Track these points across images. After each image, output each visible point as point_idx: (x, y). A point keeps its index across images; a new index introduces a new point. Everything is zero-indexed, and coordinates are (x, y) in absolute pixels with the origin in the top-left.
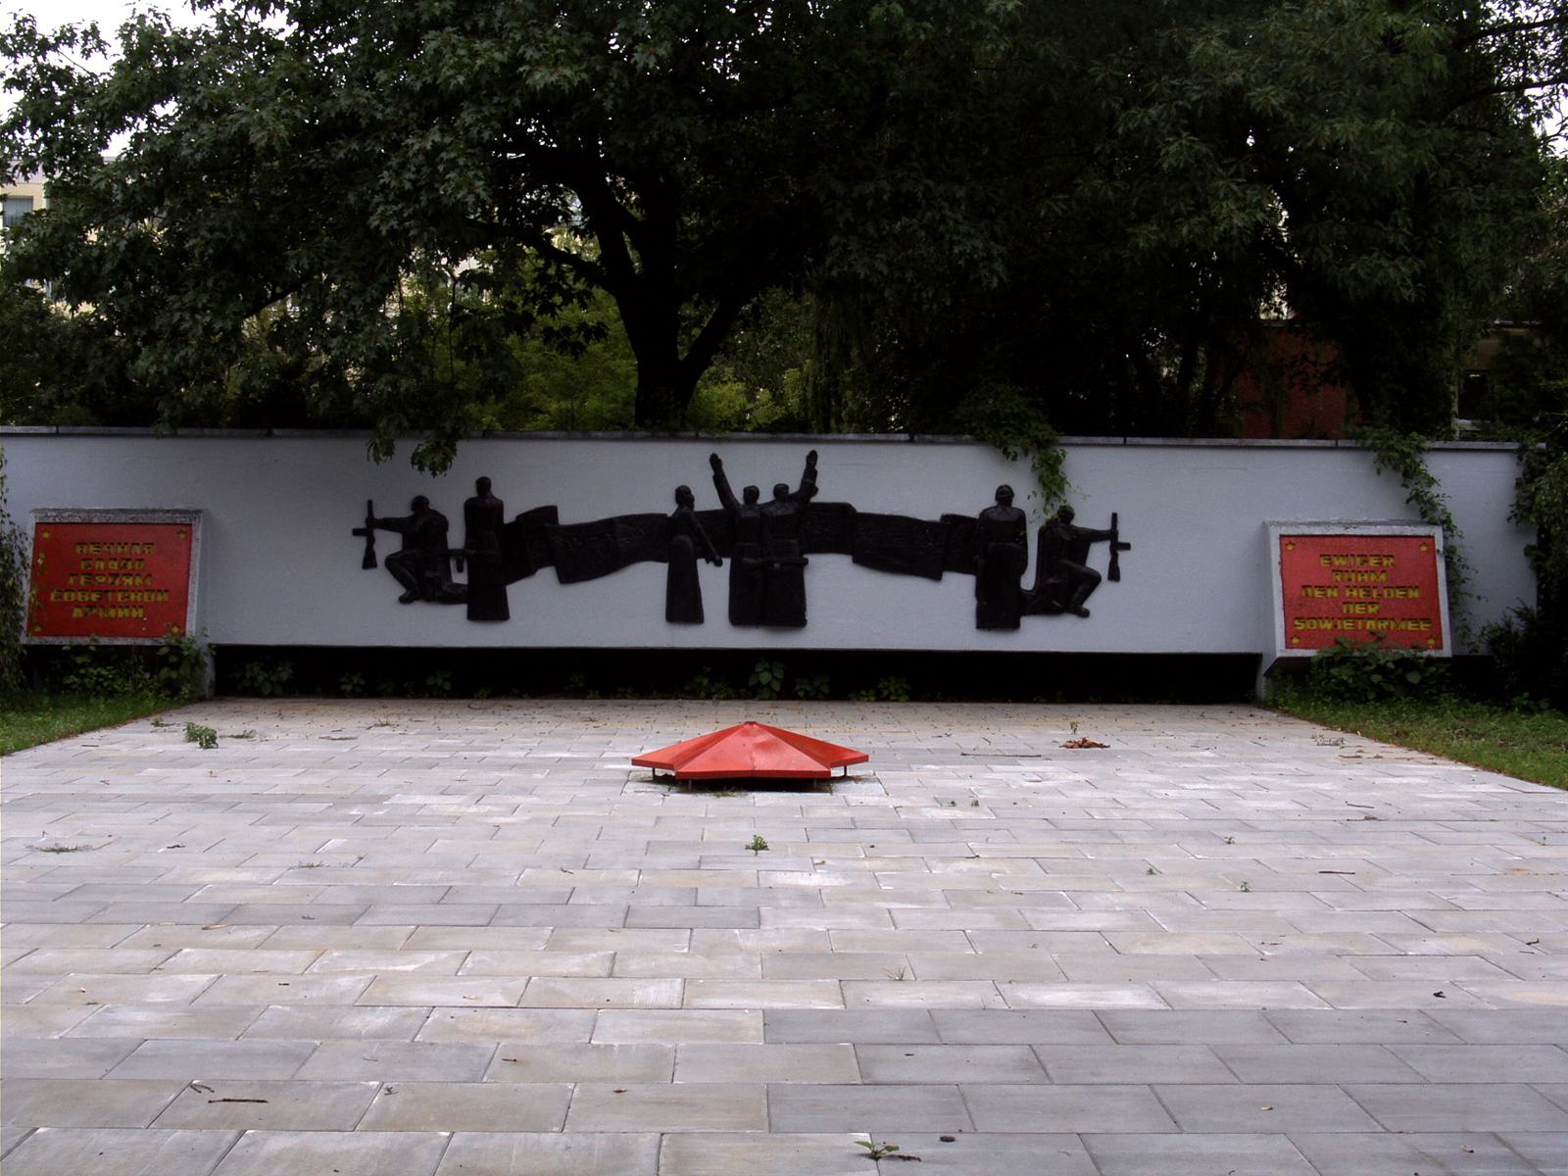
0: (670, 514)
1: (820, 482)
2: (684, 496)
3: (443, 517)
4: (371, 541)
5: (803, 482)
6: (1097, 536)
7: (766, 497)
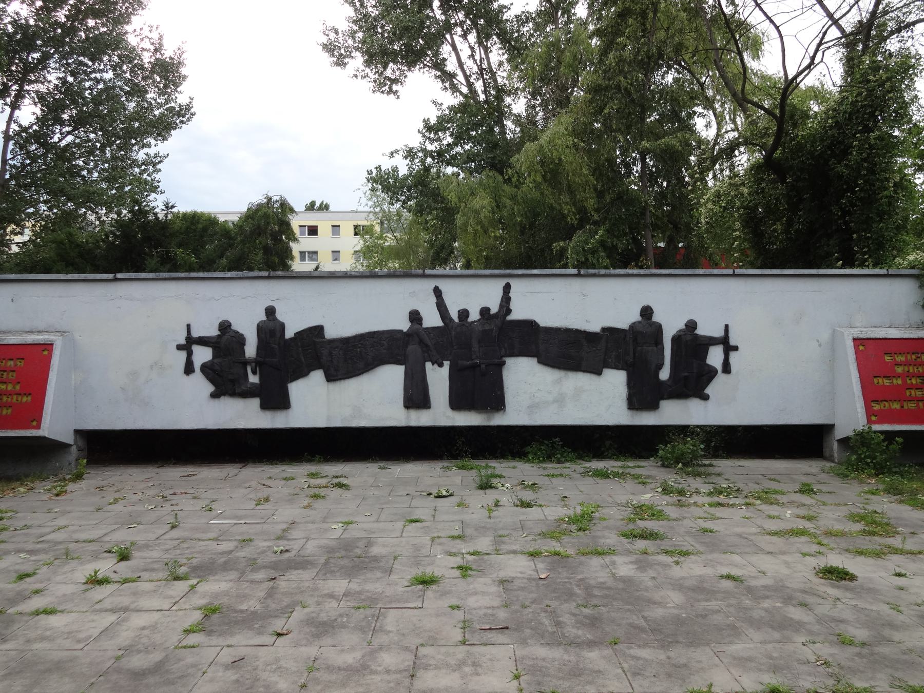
0: (405, 330)
1: (512, 306)
2: (415, 317)
3: (242, 335)
4: (190, 354)
6: (713, 341)
7: (474, 316)
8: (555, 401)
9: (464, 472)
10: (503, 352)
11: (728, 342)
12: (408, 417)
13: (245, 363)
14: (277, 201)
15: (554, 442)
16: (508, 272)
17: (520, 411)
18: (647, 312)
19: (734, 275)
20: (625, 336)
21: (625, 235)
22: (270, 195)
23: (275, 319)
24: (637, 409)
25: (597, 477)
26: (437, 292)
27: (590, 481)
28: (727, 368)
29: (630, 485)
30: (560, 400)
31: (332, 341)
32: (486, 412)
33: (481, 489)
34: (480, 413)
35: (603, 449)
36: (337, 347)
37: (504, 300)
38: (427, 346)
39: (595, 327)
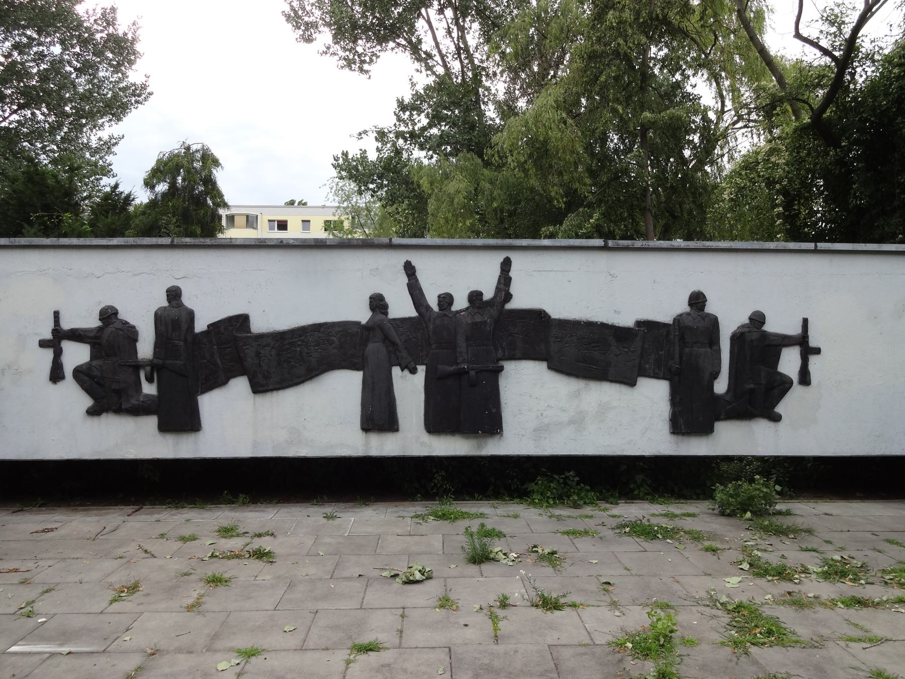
1: (513, 289)
2: (378, 303)
3: (134, 327)
4: (58, 353)
5: (498, 289)
7: (461, 303)
8: (571, 422)
9: (445, 525)
10: (500, 353)
11: (807, 342)
12: (367, 444)
13: (137, 367)
14: (197, 151)
15: (567, 477)
16: (507, 242)
17: (523, 436)
18: (697, 300)
19: (816, 251)
20: (668, 333)
21: (624, 219)
22: (188, 142)
23: (180, 305)
24: (683, 434)
25: (638, 536)
26: (409, 269)
27: (631, 546)
28: (805, 378)
29: (693, 554)
30: (578, 422)
31: (261, 336)
32: (476, 437)
33: (474, 563)
34: (468, 438)
35: (632, 486)
36: (268, 345)
37: (502, 281)
38: (394, 344)
39: (627, 320)
